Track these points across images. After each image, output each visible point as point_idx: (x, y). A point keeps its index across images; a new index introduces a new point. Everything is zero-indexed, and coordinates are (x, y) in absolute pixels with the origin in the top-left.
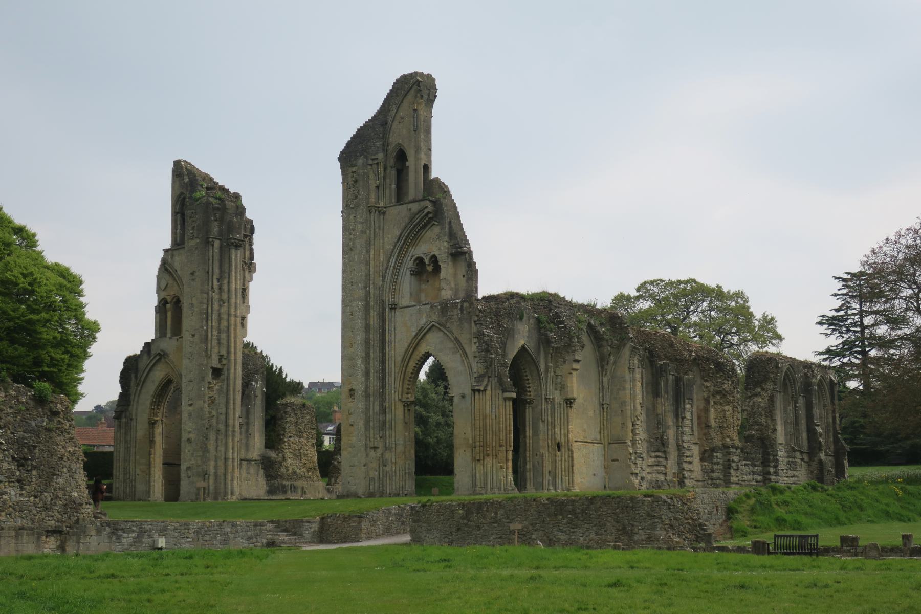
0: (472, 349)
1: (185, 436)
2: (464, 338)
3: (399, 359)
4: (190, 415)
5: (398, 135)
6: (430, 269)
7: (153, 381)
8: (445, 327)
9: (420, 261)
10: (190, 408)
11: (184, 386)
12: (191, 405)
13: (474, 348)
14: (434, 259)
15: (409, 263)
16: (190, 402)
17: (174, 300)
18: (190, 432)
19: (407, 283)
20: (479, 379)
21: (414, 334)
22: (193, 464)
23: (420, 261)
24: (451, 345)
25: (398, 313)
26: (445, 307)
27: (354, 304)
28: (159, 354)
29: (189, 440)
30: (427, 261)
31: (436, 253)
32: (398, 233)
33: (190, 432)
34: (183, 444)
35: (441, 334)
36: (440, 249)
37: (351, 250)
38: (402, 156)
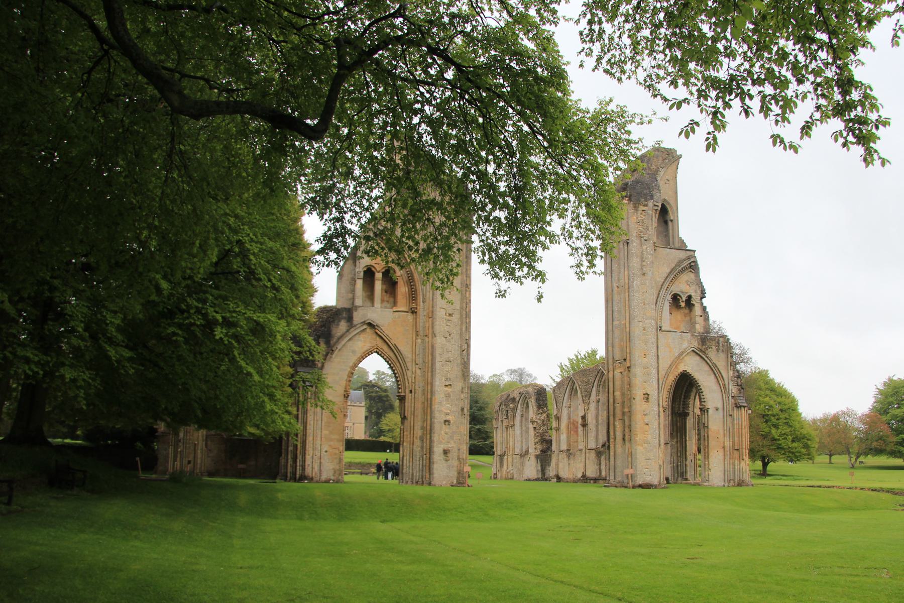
1: (439, 418)
4: (448, 396)
6: (683, 304)
7: (354, 352)
8: (704, 352)
10: (447, 389)
11: (438, 365)
12: (446, 386)
16: (448, 383)
17: (384, 270)
18: (447, 414)
21: (677, 354)
22: (453, 447)
27: (647, 321)
28: (370, 325)
31: (693, 295)
32: (668, 271)
33: (447, 414)
35: (698, 358)
36: (696, 292)
37: (644, 274)
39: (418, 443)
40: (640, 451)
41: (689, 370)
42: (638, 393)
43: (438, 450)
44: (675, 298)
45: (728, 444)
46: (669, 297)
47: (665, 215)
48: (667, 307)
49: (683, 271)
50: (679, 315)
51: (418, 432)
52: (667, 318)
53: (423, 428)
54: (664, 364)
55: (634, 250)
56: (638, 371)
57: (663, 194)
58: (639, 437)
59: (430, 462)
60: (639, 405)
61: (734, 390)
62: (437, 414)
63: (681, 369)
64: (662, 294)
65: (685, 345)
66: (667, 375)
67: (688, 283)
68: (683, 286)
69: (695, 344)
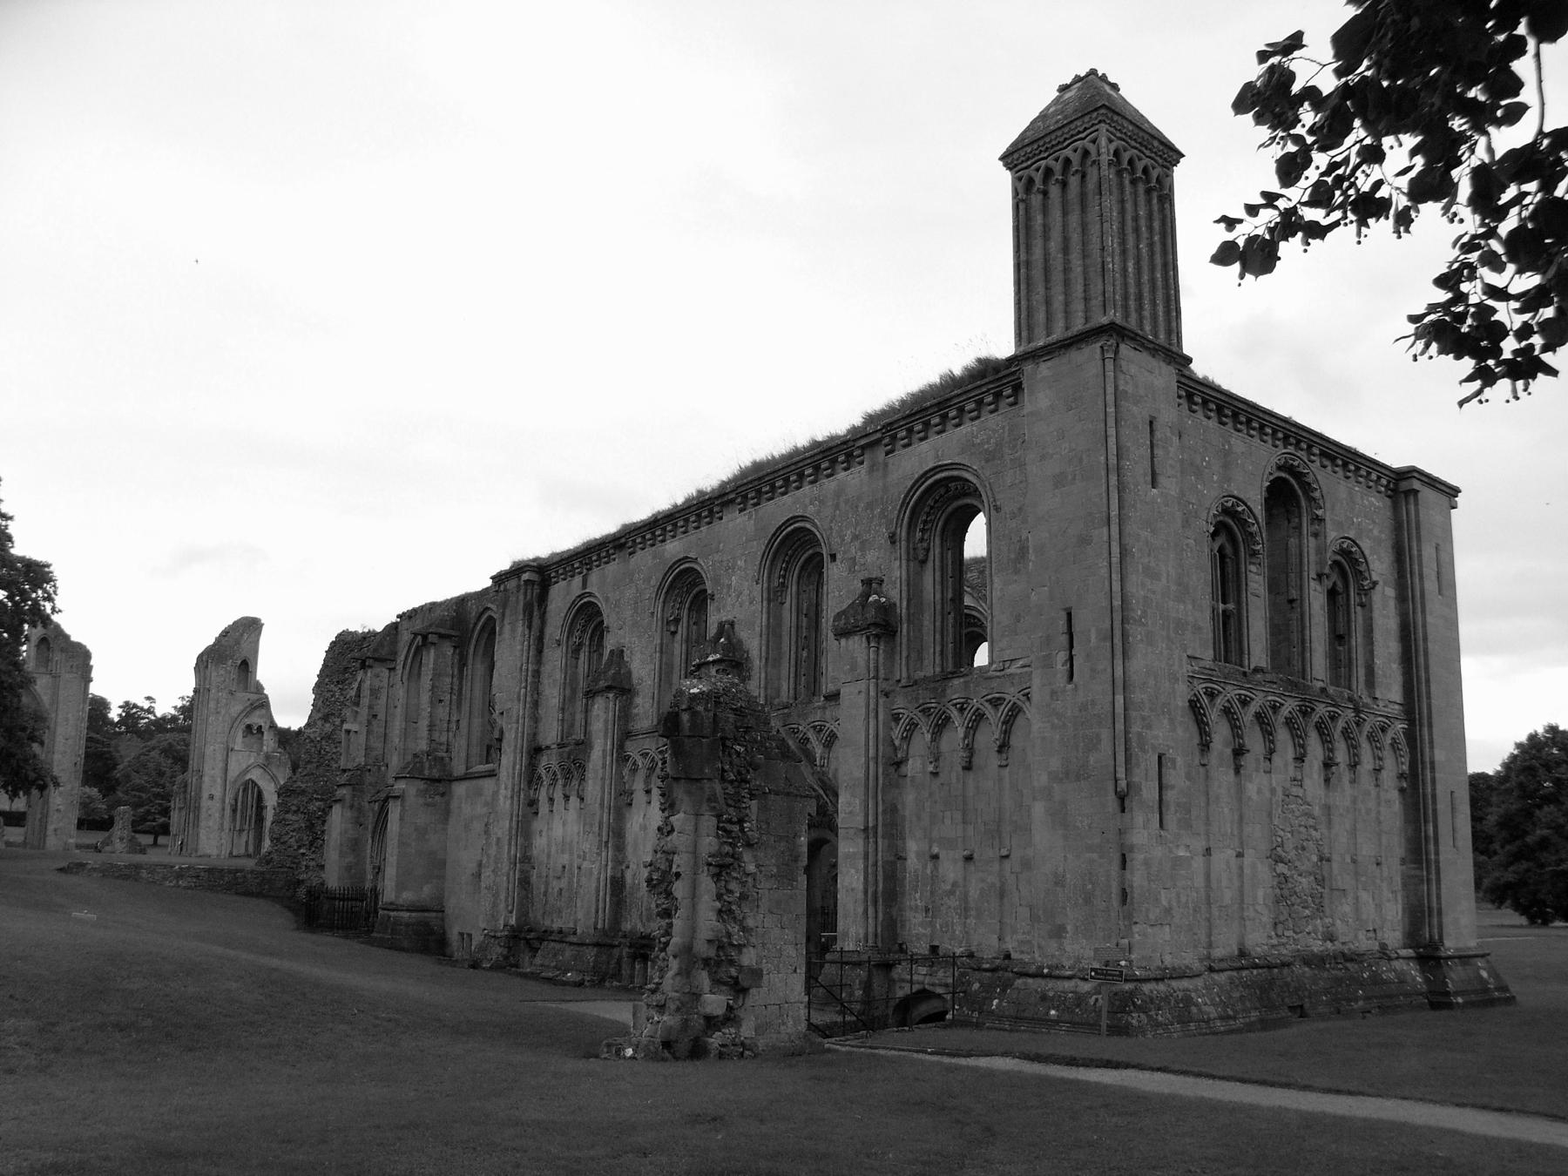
29: (58, 810)
32: (242, 708)
34: (51, 813)
35: (262, 770)
39: (37, 823)
40: (203, 833)
41: (254, 778)
42: (205, 795)
43: (51, 828)
44: (249, 727)
46: (243, 727)
47: (246, 667)
48: (240, 734)
49: (255, 708)
50: (252, 739)
51: (39, 816)
52: (239, 741)
53: (41, 813)
54: (234, 770)
55: (211, 696)
56: (206, 779)
57: (244, 652)
58: (203, 824)
59: (45, 836)
60: (205, 803)
62: (51, 805)
63: (247, 777)
64: (235, 725)
65: (252, 760)
66: (236, 781)
67: (261, 717)
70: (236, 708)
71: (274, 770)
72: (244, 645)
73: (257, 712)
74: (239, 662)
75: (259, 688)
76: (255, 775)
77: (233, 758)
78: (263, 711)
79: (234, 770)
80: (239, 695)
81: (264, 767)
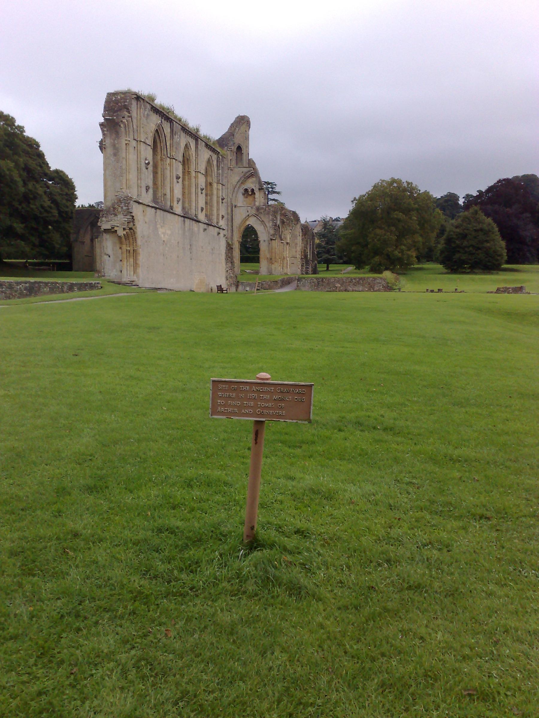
0: (270, 224)
2: (266, 220)
3: (238, 226)
5: (238, 139)
6: (250, 193)
9: (246, 190)
13: (271, 224)
14: (253, 190)
15: (242, 191)
19: (240, 197)
20: (273, 235)
23: (246, 190)
24: (260, 222)
25: (237, 208)
26: (258, 209)
30: (250, 191)
38: (239, 148)
45: (268, 256)
49: (249, 177)
50: (250, 199)
52: (240, 200)
54: (237, 221)
61: (272, 232)
63: (247, 223)
66: (240, 228)
67: (252, 183)
68: (250, 184)
69: (254, 212)
70: (235, 178)
71: (262, 217)
72: (236, 136)
73: (251, 180)
74: (234, 148)
75: (251, 164)
76: (252, 222)
77: (236, 211)
78: (254, 179)
79: (237, 221)
80: (237, 170)
81: (255, 216)
